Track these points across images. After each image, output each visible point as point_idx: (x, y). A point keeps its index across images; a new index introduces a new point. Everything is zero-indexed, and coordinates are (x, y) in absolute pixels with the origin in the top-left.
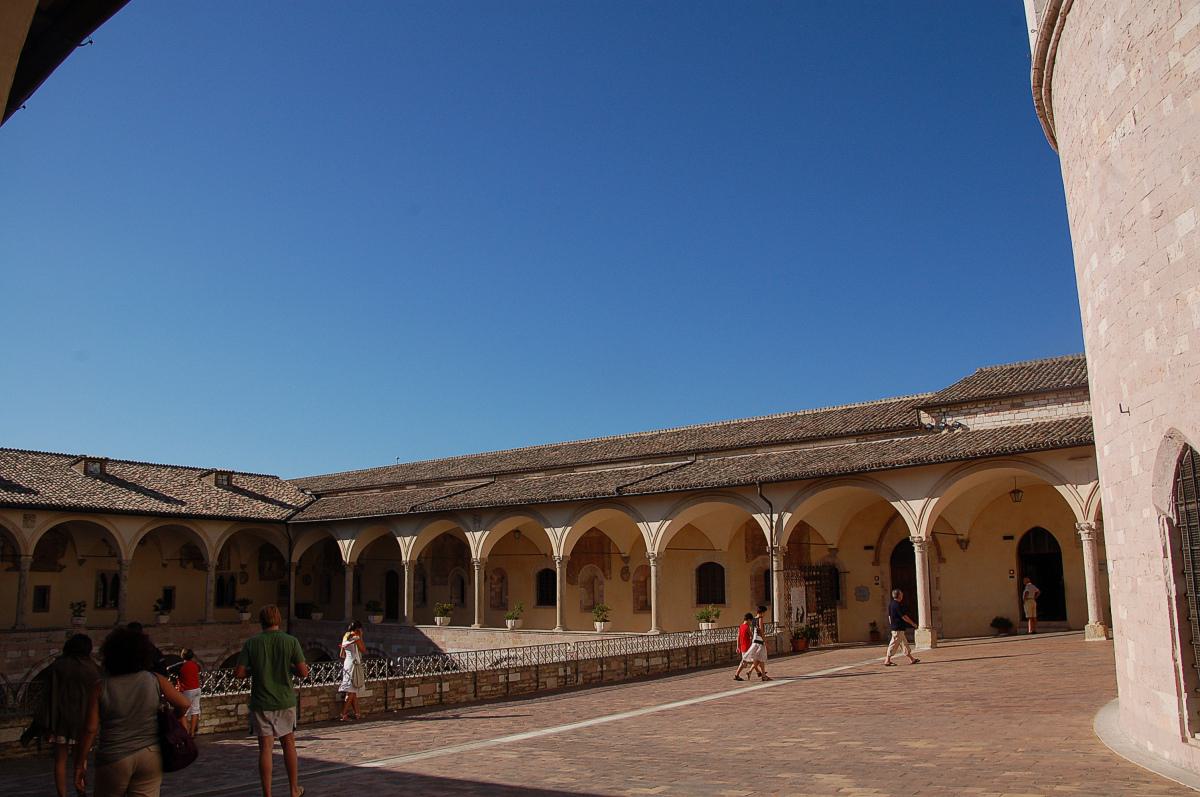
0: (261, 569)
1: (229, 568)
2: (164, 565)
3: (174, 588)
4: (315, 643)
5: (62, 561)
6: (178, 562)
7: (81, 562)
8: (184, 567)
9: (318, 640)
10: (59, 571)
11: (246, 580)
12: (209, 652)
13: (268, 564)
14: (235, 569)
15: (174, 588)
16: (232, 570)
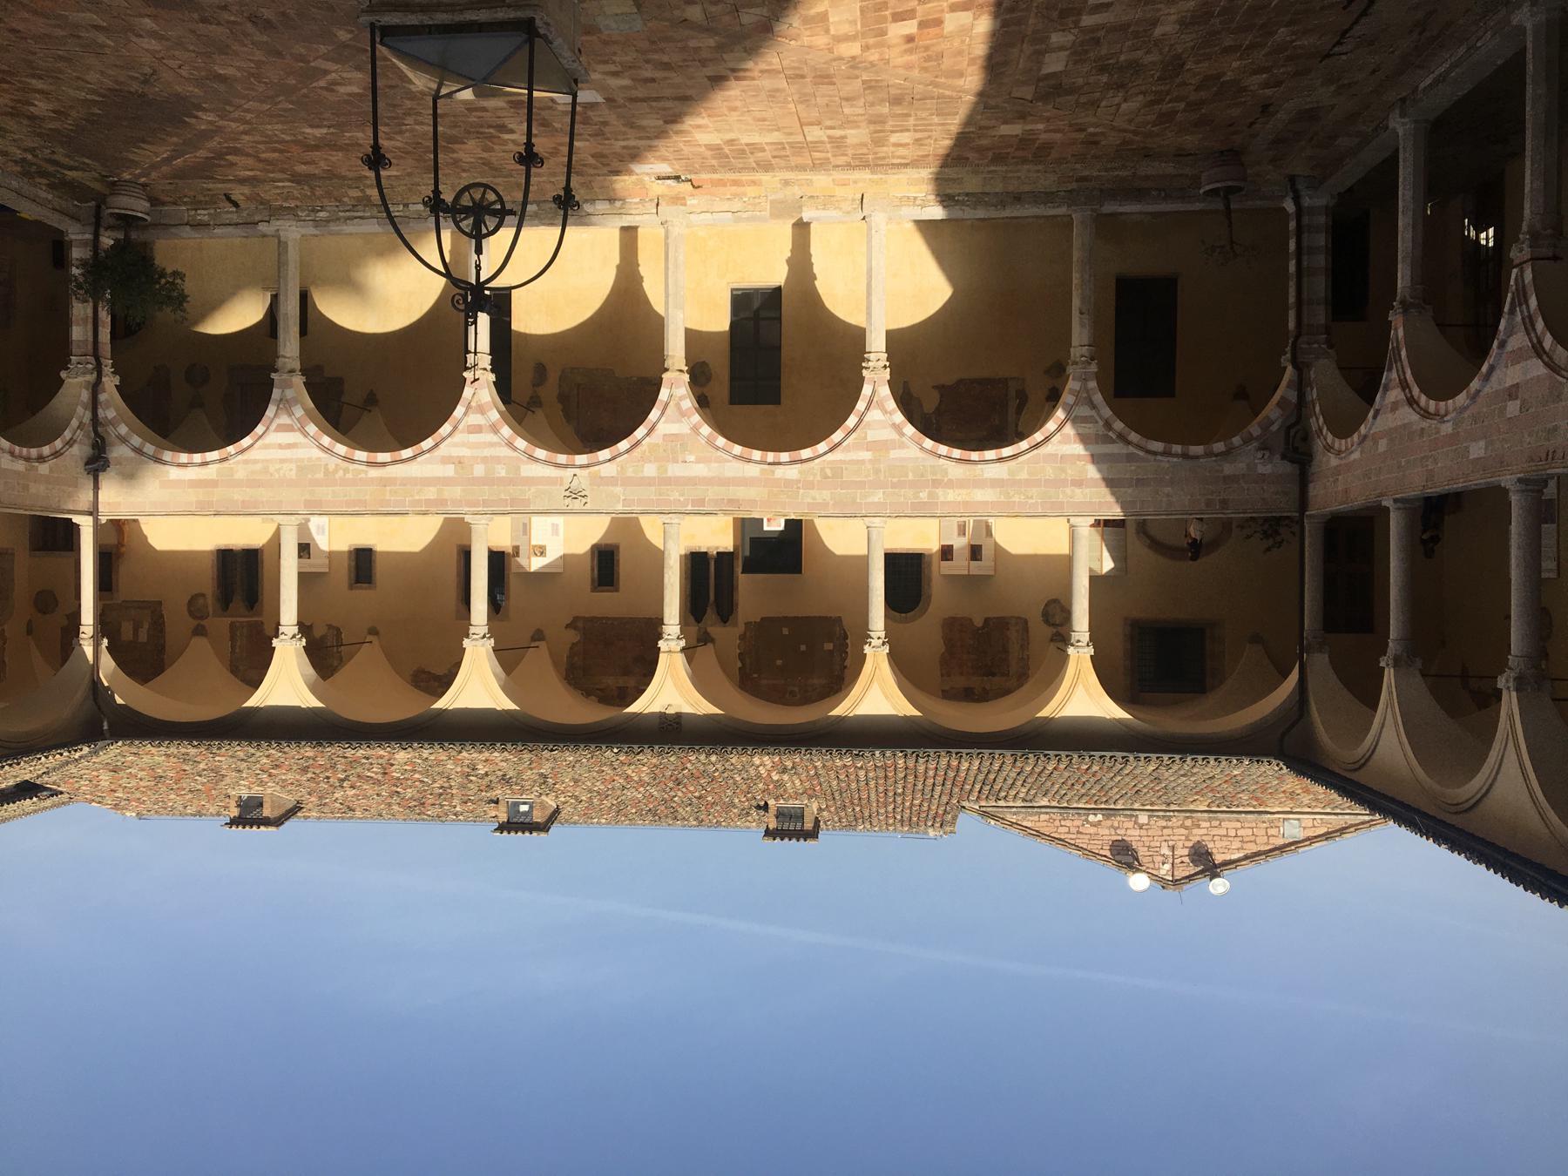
0: (158, 625)
1: (232, 625)
2: (373, 631)
3: (351, 588)
4: (28, 459)
5: (573, 636)
6: (345, 638)
7: (538, 636)
8: (330, 627)
9: (20, 466)
10: (576, 619)
11: (192, 601)
12: (287, 454)
13: (143, 636)
14: (220, 624)
15: (351, 588)
16: (229, 620)
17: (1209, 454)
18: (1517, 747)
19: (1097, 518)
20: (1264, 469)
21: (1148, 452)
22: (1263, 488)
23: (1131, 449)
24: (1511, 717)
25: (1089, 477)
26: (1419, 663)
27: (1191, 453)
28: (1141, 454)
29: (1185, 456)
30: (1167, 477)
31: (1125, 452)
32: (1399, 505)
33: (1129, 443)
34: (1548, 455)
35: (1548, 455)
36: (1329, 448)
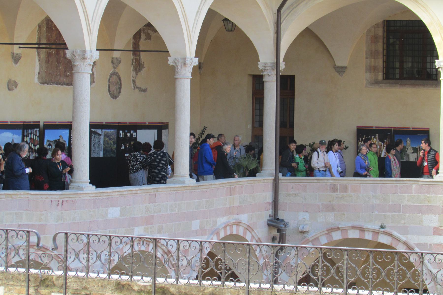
17: (344, 230)
18: (85, 12)
19: (431, 180)
20: (304, 216)
21: (390, 235)
22: (305, 199)
23: (404, 238)
24: (90, 32)
25: (437, 216)
26: (171, 62)
27: (357, 231)
28: (395, 233)
29: (362, 230)
30: (376, 212)
31: (409, 236)
32: (181, 179)
33: (405, 243)
34: (62, 204)
35: (62, 204)
36: (249, 228)
